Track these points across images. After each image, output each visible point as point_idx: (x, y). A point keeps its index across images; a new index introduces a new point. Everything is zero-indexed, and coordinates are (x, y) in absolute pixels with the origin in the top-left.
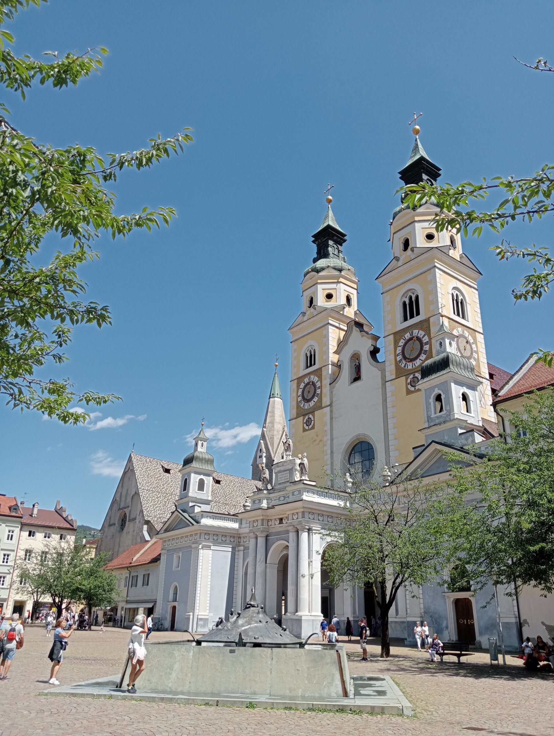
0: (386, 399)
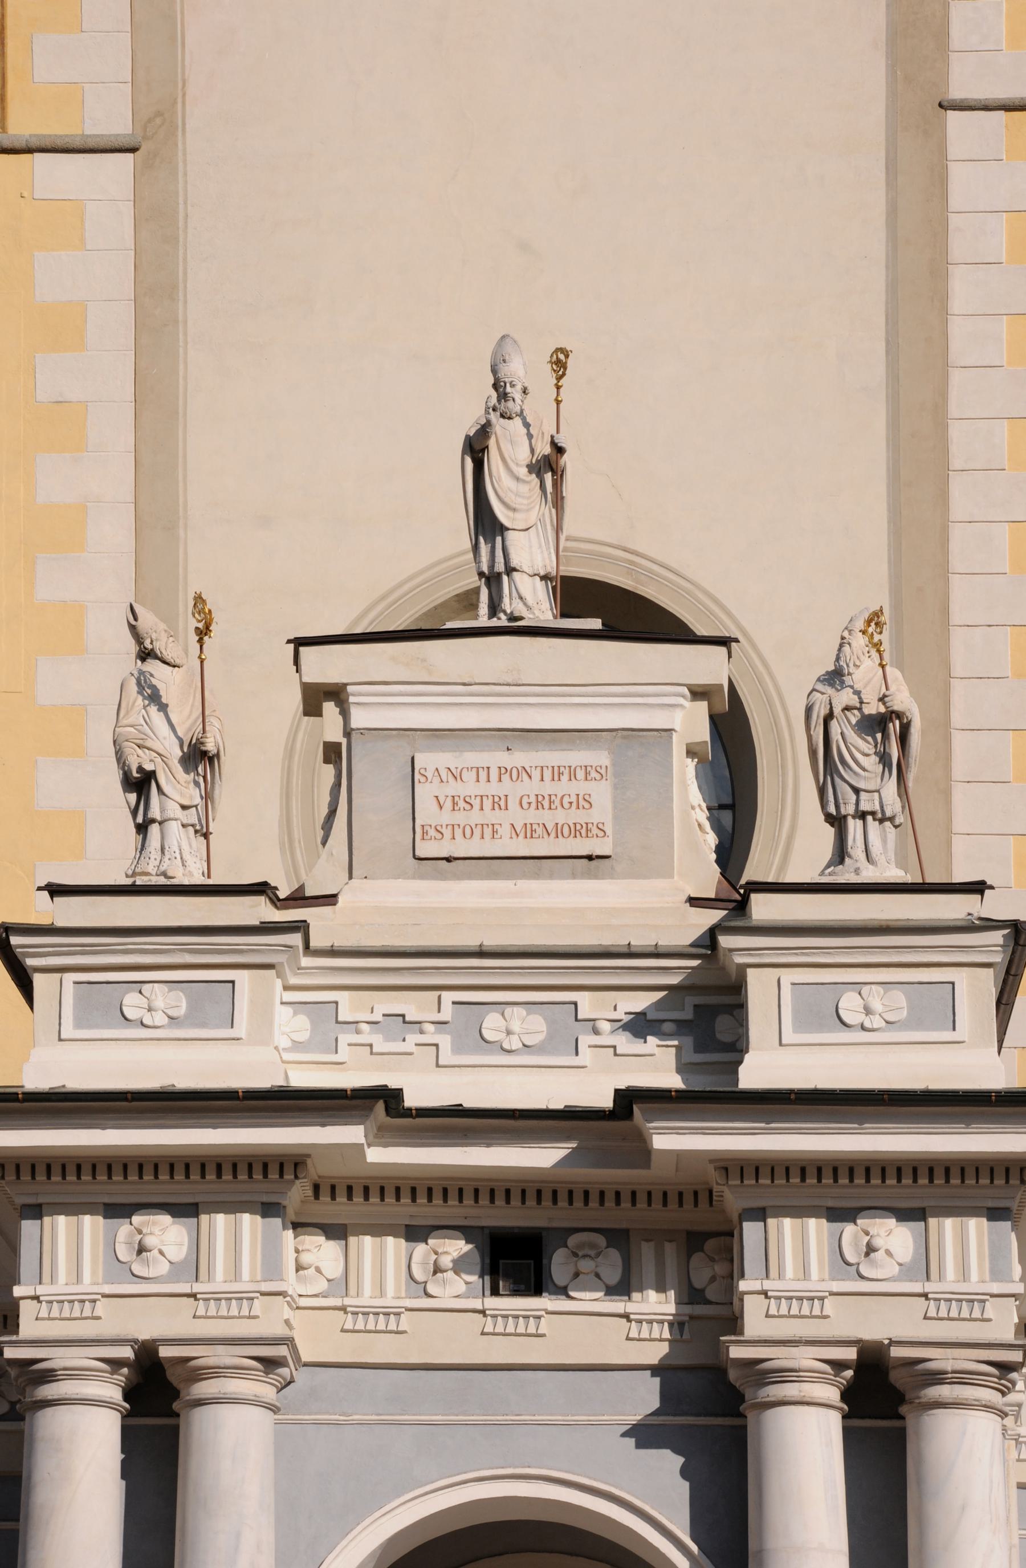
0: (939, 270)
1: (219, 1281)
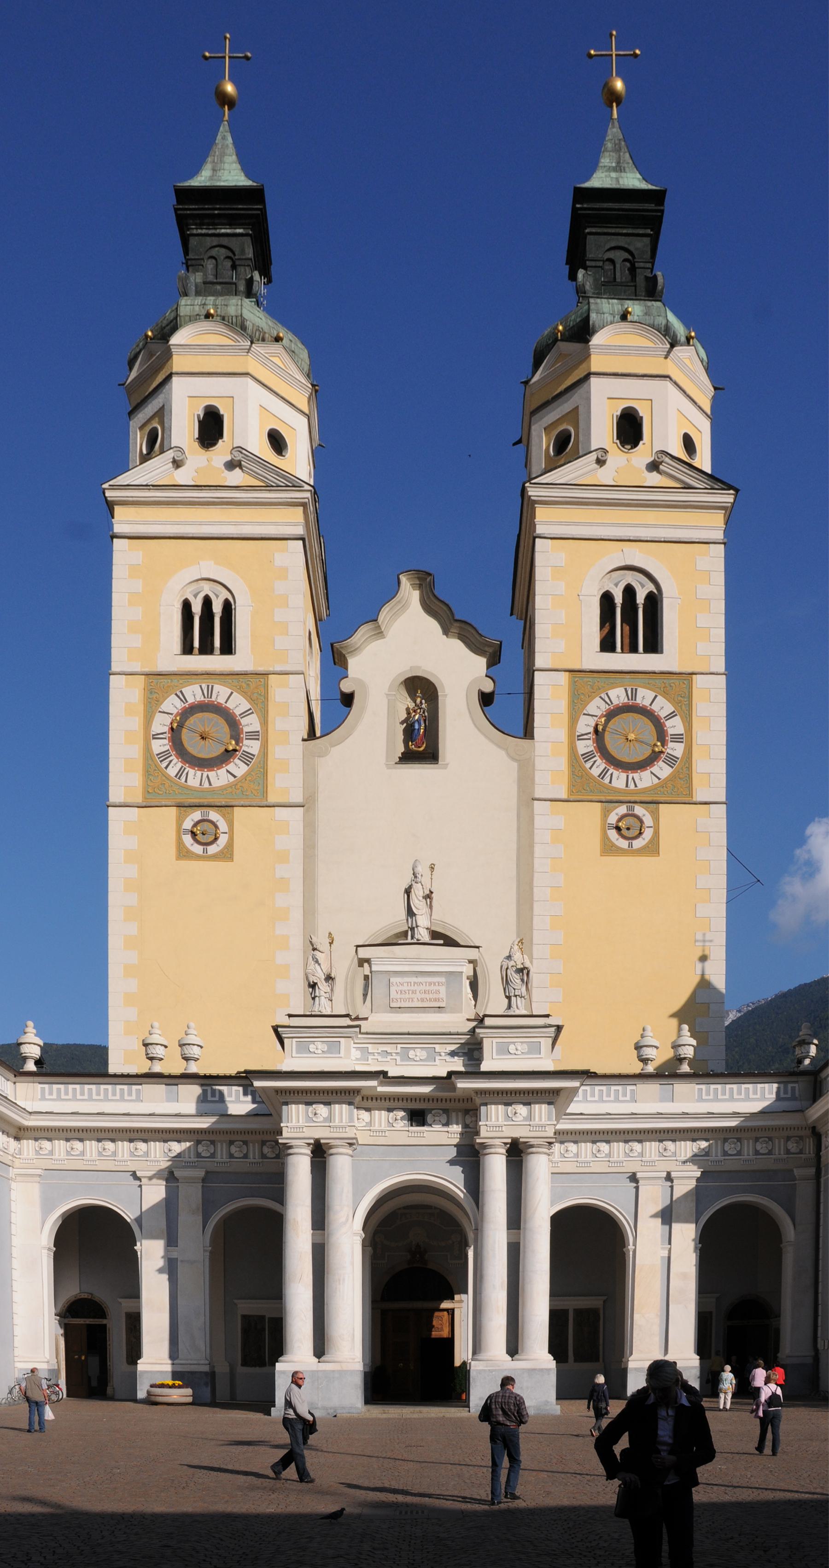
1: (337, 1122)
